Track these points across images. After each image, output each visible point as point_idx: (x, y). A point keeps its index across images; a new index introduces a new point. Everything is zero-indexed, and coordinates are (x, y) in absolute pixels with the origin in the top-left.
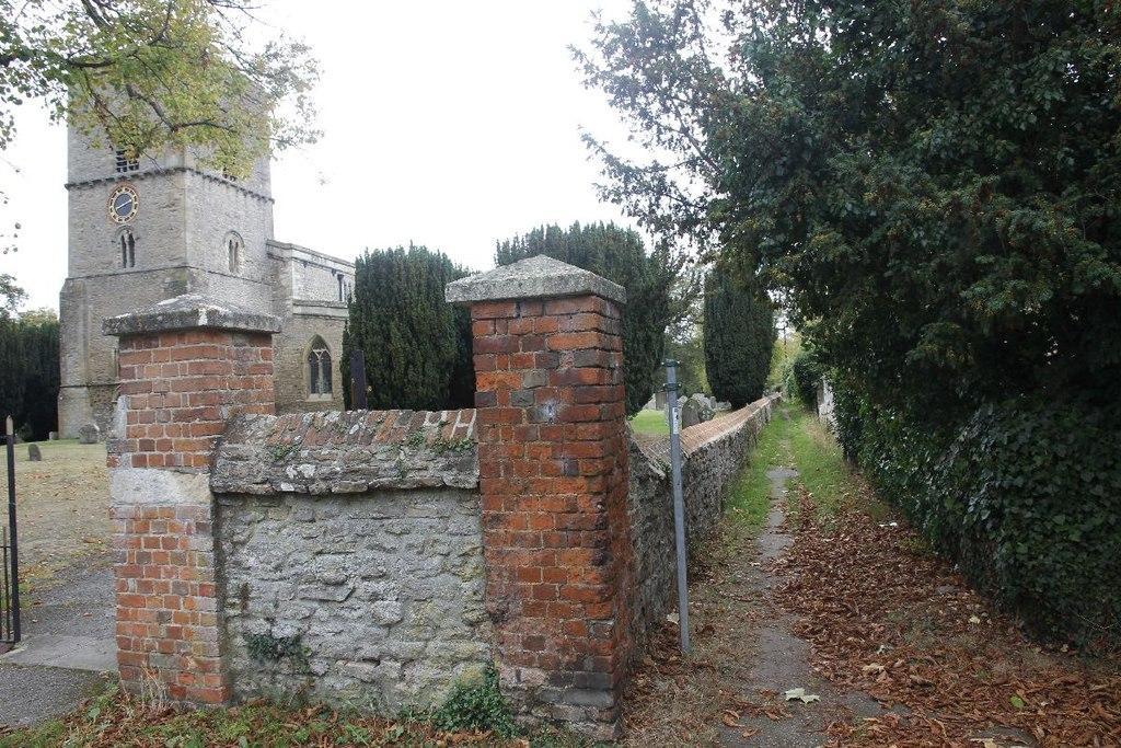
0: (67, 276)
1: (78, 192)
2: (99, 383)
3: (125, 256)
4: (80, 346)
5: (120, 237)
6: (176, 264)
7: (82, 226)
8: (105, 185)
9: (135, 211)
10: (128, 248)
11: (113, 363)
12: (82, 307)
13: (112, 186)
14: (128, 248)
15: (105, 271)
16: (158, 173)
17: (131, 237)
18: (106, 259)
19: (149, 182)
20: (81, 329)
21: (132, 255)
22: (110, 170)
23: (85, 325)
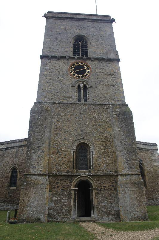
0: (36, 101)
1: (49, 61)
2: (58, 173)
3: (79, 96)
4: (46, 145)
5: (77, 85)
6: (118, 103)
7: (50, 76)
8: (68, 60)
9: (87, 74)
10: (82, 91)
11: (72, 159)
12: (49, 120)
13: (71, 62)
14: (82, 91)
15: (65, 101)
16: (103, 59)
17: (85, 87)
18: (67, 95)
19: (96, 62)
20: (47, 134)
21: (85, 96)
22: (71, 54)
23: (50, 132)
